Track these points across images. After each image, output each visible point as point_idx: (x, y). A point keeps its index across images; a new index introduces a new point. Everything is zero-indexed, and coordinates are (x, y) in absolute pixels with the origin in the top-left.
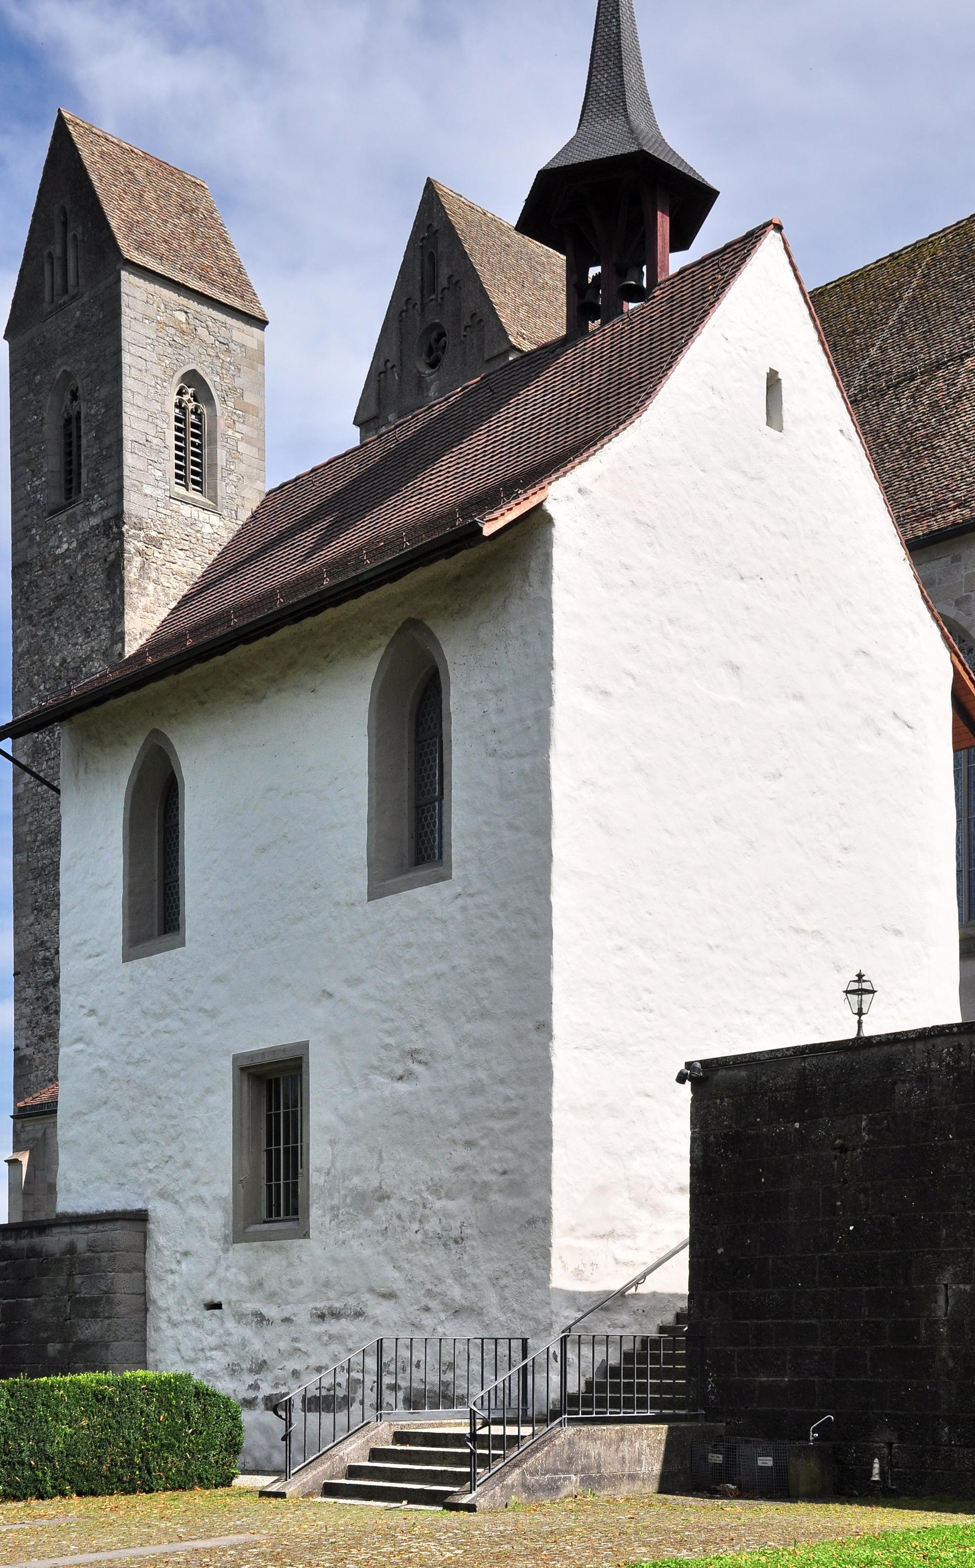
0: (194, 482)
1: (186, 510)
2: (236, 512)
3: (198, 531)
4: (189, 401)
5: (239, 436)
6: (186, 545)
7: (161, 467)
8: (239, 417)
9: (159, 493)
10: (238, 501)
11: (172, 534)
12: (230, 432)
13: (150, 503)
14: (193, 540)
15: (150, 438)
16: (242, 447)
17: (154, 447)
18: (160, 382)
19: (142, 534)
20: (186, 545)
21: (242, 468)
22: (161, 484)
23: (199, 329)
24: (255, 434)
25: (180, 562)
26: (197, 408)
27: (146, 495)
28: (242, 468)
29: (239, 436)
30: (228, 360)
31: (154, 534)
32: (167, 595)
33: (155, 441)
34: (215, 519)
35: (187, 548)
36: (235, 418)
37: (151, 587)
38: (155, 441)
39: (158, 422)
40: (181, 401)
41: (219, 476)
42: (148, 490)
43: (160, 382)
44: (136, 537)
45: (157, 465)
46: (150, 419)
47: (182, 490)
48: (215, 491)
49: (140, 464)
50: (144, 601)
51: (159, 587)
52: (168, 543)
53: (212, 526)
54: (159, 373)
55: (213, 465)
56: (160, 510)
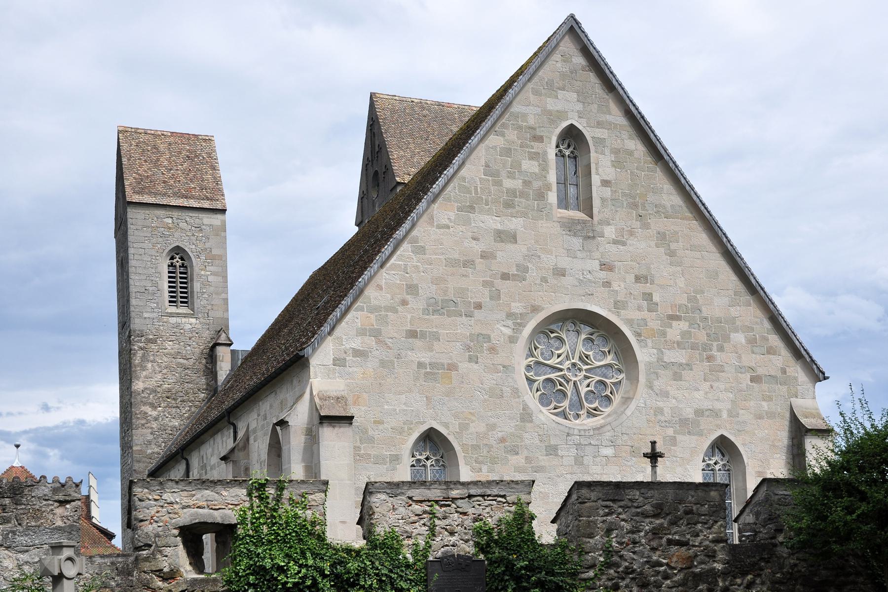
0: (182, 302)
1: (173, 320)
2: (208, 314)
3: (181, 329)
4: (177, 262)
5: (209, 273)
6: (174, 338)
7: (155, 301)
8: (209, 263)
9: (155, 315)
10: (209, 307)
11: (163, 334)
12: (203, 273)
13: (148, 321)
14: (178, 334)
15: (147, 288)
16: (211, 278)
17: (150, 292)
18: (154, 258)
19: (143, 339)
20: (174, 338)
21: (212, 289)
22: (156, 310)
23: (181, 225)
24: (220, 269)
25: (169, 348)
26: (183, 264)
27: (145, 318)
28: (212, 289)
29: (209, 273)
30: (201, 235)
31: (151, 337)
32: (160, 367)
33: (151, 289)
34: (193, 320)
35: (174, 339)
36: (207, 264)
37: (149, 365)
38: (151, 289)
39: (153, 278)
40: (172, 263)
41: (195, 297)
42: (146, 315)
43: (154, 258)
44: (140, 341)
45: (153, 301)
46: (148, 278)
47: (173, 309)
48: (194, 305)
49: (141, 303)
50: (144, 373)
51: (155, 364)
52: (161, 339)
53: (191, 324)
54: (153, 252)
55: (192, 292)
56: (155, 323)
